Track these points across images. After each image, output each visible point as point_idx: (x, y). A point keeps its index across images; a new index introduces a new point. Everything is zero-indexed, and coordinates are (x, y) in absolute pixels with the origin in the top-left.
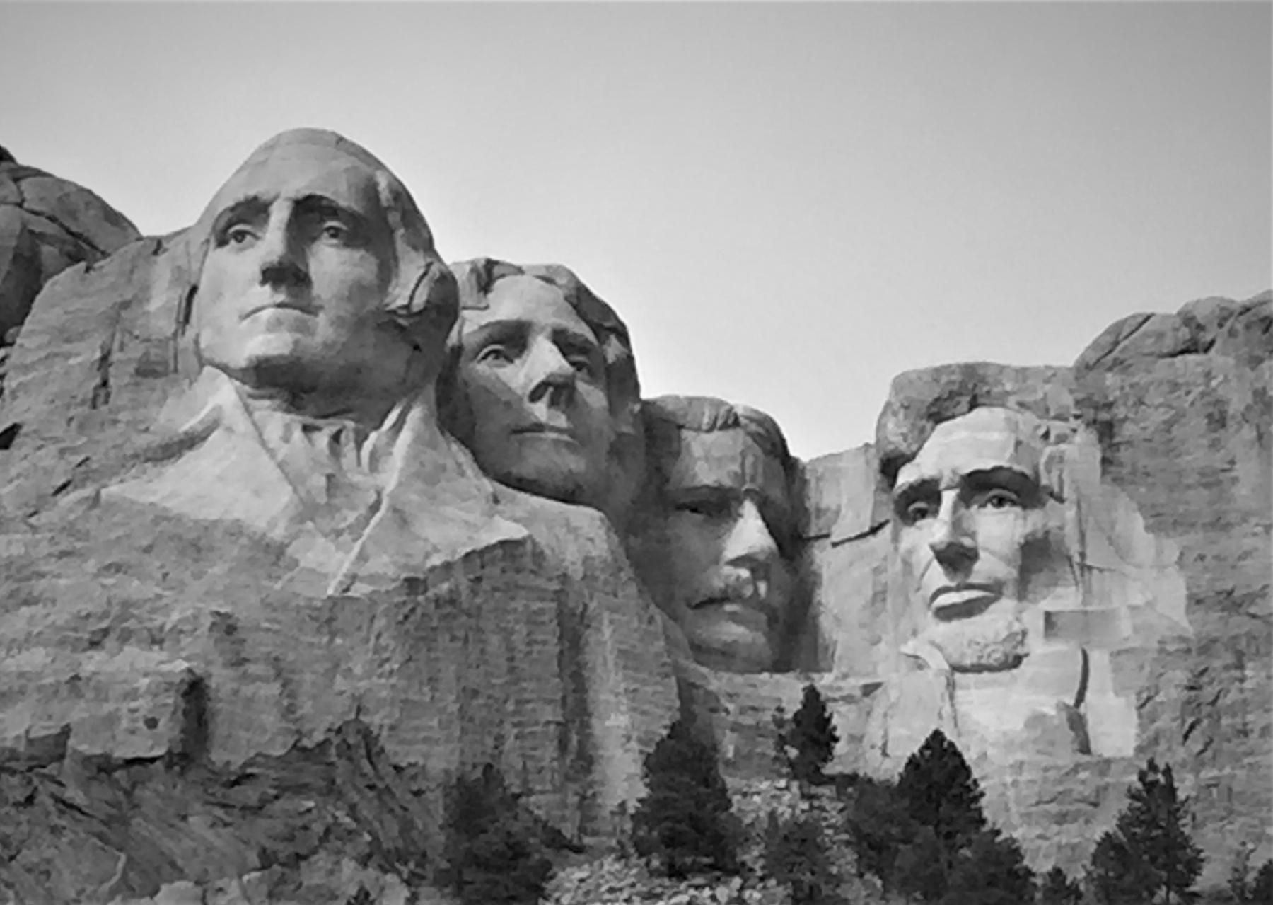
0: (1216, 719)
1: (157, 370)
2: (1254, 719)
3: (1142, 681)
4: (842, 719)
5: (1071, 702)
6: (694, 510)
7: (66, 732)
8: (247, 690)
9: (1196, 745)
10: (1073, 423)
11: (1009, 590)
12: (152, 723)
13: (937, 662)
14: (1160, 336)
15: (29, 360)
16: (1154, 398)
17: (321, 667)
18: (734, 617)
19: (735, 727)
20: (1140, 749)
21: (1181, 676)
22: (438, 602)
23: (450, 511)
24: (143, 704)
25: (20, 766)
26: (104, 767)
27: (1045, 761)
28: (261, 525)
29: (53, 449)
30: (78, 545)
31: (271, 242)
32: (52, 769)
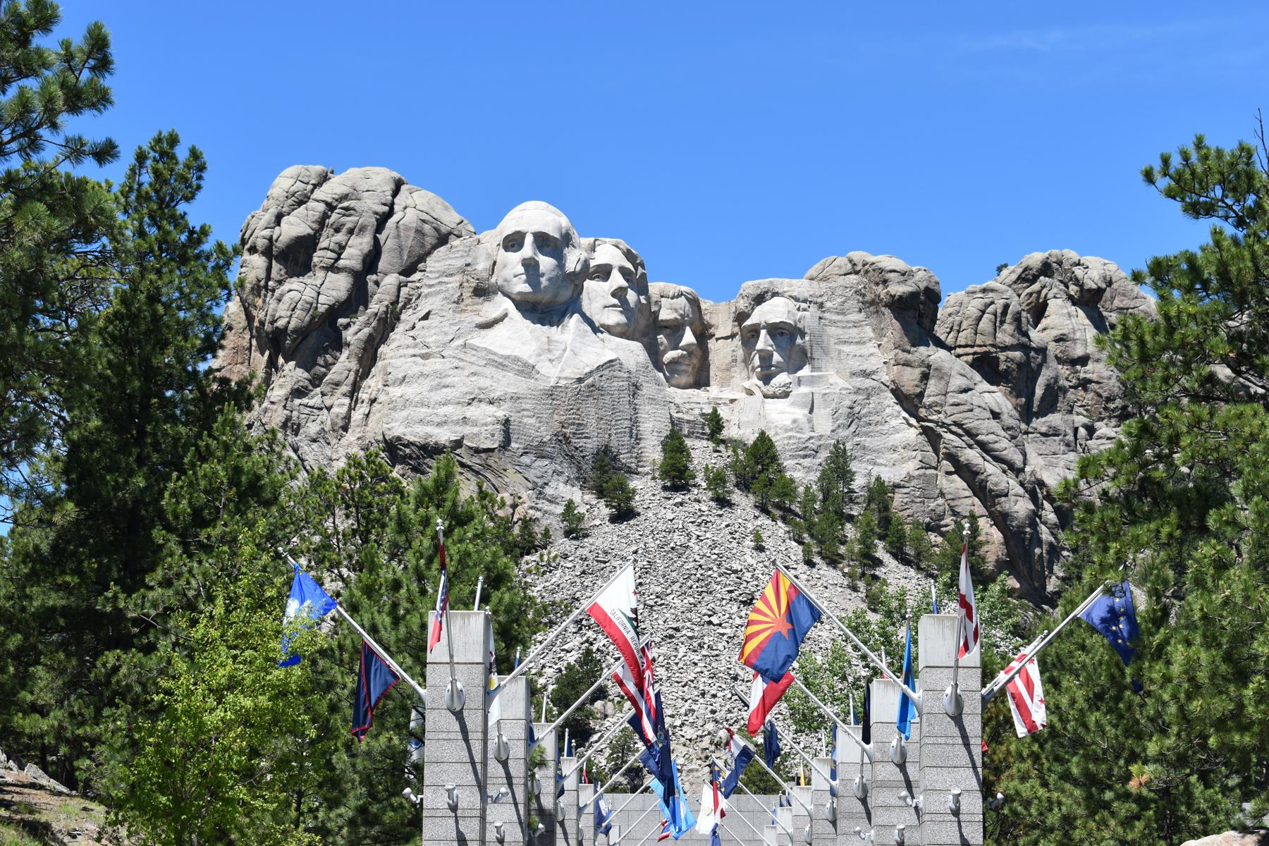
0: (860, 419)
1: (482, 292)
2: (875, 418)
4: (723, 412)
5: (807, 411)
8: (525, 420)
12: (493, 435)
13: (758, 394)
14: (840, 267)
15: (432, 282)
16: (839, 292)
19: (688, 422)
20: (833, 431)
21: (848, 403)
22: (588, 386)
23: (590, 349)
24: (490, 427)
26: (477, 451)
27: (799, 435)
28: (525, 357)
29: (447, 323)
30: (461, 364)
32: (458, 451)
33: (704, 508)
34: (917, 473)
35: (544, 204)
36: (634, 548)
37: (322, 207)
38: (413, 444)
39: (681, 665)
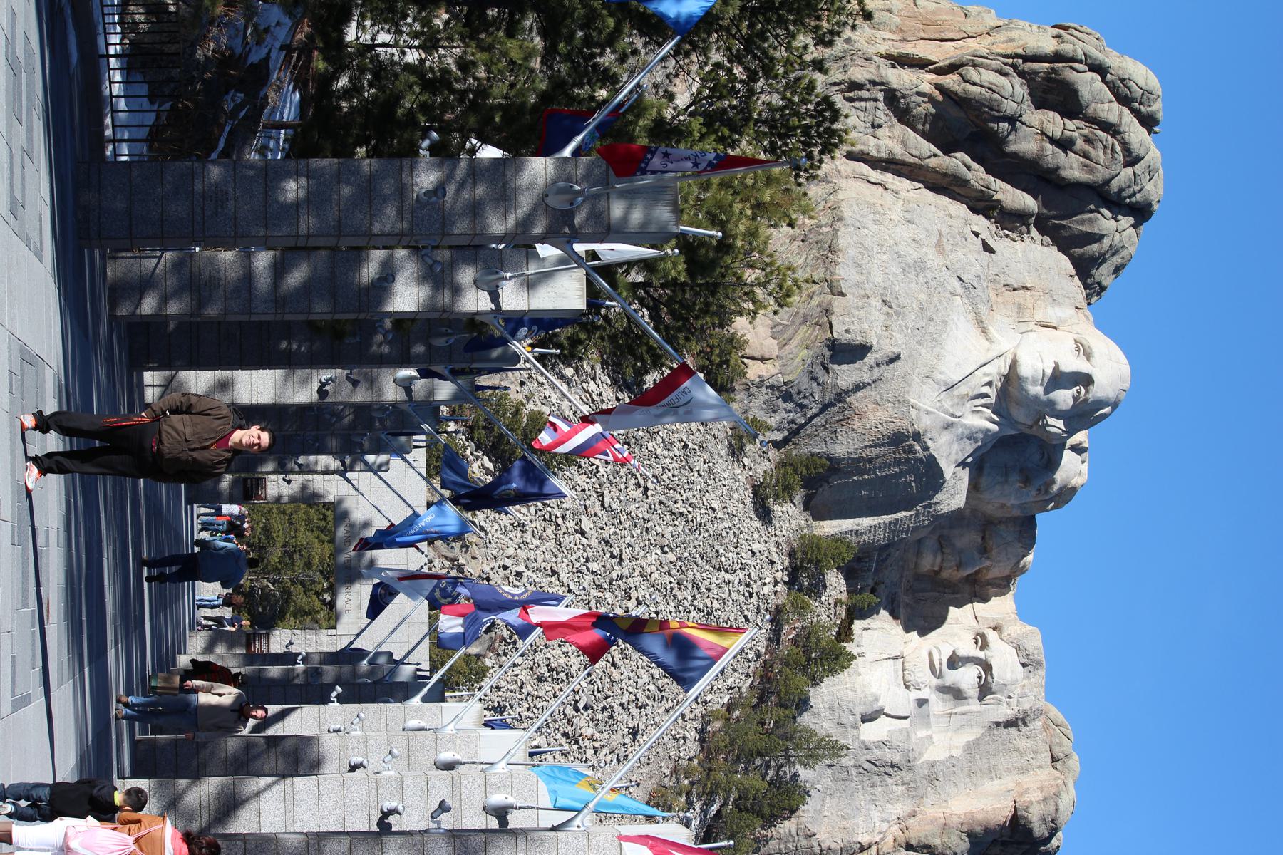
3: (895, 742)
6: (983, 538)
7: (843, 295)
9: (867, 766)
10: (1016, 709)
11: (939, 682)
12: (847, 331)
14: (1060, 745)
16: (1030, 744)
17: (878, 398)
18: (935, 557)
20: (863, 742)
21: (897, 758)
25: (828, 277)
26: (827, 312)
31: (1073, 364)
33: (766, 590)
34: (815, 844)
35: (1126, 386)
36: (715, 505)
37: (1113, 118)
38: (835, 236)
39: (577, 565)
